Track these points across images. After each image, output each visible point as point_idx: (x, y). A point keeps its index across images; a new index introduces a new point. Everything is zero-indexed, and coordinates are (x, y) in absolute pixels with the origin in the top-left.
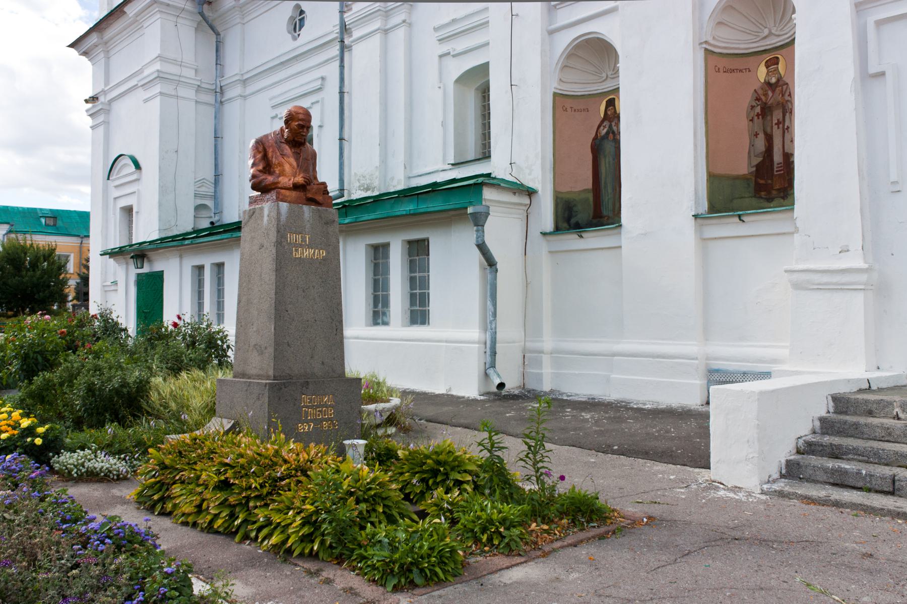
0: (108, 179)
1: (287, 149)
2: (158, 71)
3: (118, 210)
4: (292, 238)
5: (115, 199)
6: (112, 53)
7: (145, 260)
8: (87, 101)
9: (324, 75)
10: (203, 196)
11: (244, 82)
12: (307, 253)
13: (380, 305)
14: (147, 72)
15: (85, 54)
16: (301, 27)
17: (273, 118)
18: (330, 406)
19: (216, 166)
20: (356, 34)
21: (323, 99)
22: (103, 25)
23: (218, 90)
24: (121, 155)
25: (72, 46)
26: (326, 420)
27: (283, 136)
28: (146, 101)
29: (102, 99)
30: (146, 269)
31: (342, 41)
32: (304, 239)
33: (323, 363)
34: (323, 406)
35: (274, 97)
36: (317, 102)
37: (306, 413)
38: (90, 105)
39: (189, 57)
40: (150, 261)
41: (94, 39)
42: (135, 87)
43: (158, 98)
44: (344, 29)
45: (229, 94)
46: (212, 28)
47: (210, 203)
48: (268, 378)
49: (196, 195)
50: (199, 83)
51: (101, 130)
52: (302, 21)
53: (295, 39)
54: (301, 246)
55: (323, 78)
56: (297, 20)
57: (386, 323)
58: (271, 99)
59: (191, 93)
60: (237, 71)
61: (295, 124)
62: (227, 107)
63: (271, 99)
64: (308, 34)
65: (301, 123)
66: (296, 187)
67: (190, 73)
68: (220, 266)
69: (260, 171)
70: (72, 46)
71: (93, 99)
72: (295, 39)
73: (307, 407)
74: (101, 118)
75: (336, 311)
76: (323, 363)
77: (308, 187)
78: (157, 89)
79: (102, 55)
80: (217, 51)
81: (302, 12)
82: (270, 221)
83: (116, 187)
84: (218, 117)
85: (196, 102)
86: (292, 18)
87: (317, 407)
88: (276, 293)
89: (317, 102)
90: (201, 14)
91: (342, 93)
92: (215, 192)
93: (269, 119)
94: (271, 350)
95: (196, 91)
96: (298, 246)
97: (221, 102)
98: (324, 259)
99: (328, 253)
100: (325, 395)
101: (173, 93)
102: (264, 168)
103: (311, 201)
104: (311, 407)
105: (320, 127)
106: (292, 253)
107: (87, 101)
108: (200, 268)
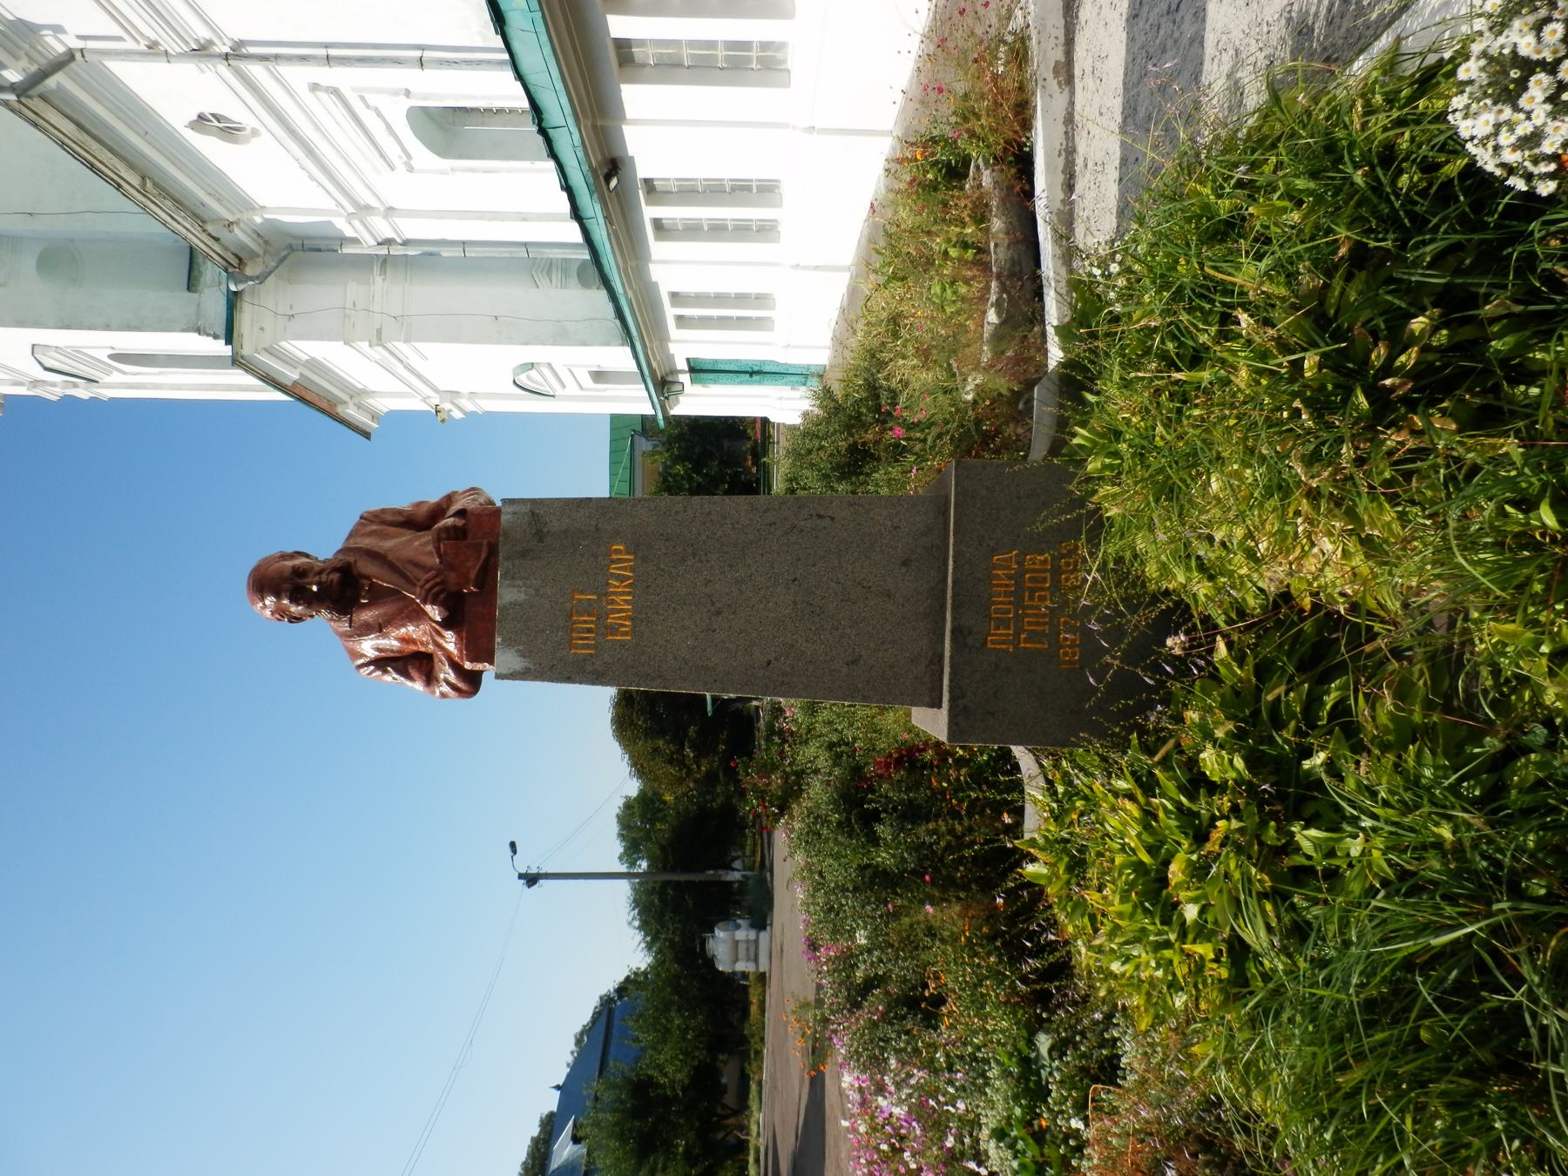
7: (670, 379)
12: (622, 601)
14: (377, 357)
16: (228, 120)
17: (411, 169)
20: (203, 33)
21: (354, 89)
22: (324, 405)
31: (226, 57)
32: (588, 609)
33: (905, 563)
36: (362, 98)
37: (1033, 636)
44: (202, 51)
52: (217, 117)
53: (255, 133)
54: (602, 616)
68: (675, 297)
73: (1017, 635)
76: (905, 563)
79: (370, 401)
83: (564, 386)
87: (1019, 603)
89: (362, 98)
98: (635, 547)
102: (420, 671)
103: (486, 580)
105: (408, 93)
106: (622, 644)
108: (680, 320)
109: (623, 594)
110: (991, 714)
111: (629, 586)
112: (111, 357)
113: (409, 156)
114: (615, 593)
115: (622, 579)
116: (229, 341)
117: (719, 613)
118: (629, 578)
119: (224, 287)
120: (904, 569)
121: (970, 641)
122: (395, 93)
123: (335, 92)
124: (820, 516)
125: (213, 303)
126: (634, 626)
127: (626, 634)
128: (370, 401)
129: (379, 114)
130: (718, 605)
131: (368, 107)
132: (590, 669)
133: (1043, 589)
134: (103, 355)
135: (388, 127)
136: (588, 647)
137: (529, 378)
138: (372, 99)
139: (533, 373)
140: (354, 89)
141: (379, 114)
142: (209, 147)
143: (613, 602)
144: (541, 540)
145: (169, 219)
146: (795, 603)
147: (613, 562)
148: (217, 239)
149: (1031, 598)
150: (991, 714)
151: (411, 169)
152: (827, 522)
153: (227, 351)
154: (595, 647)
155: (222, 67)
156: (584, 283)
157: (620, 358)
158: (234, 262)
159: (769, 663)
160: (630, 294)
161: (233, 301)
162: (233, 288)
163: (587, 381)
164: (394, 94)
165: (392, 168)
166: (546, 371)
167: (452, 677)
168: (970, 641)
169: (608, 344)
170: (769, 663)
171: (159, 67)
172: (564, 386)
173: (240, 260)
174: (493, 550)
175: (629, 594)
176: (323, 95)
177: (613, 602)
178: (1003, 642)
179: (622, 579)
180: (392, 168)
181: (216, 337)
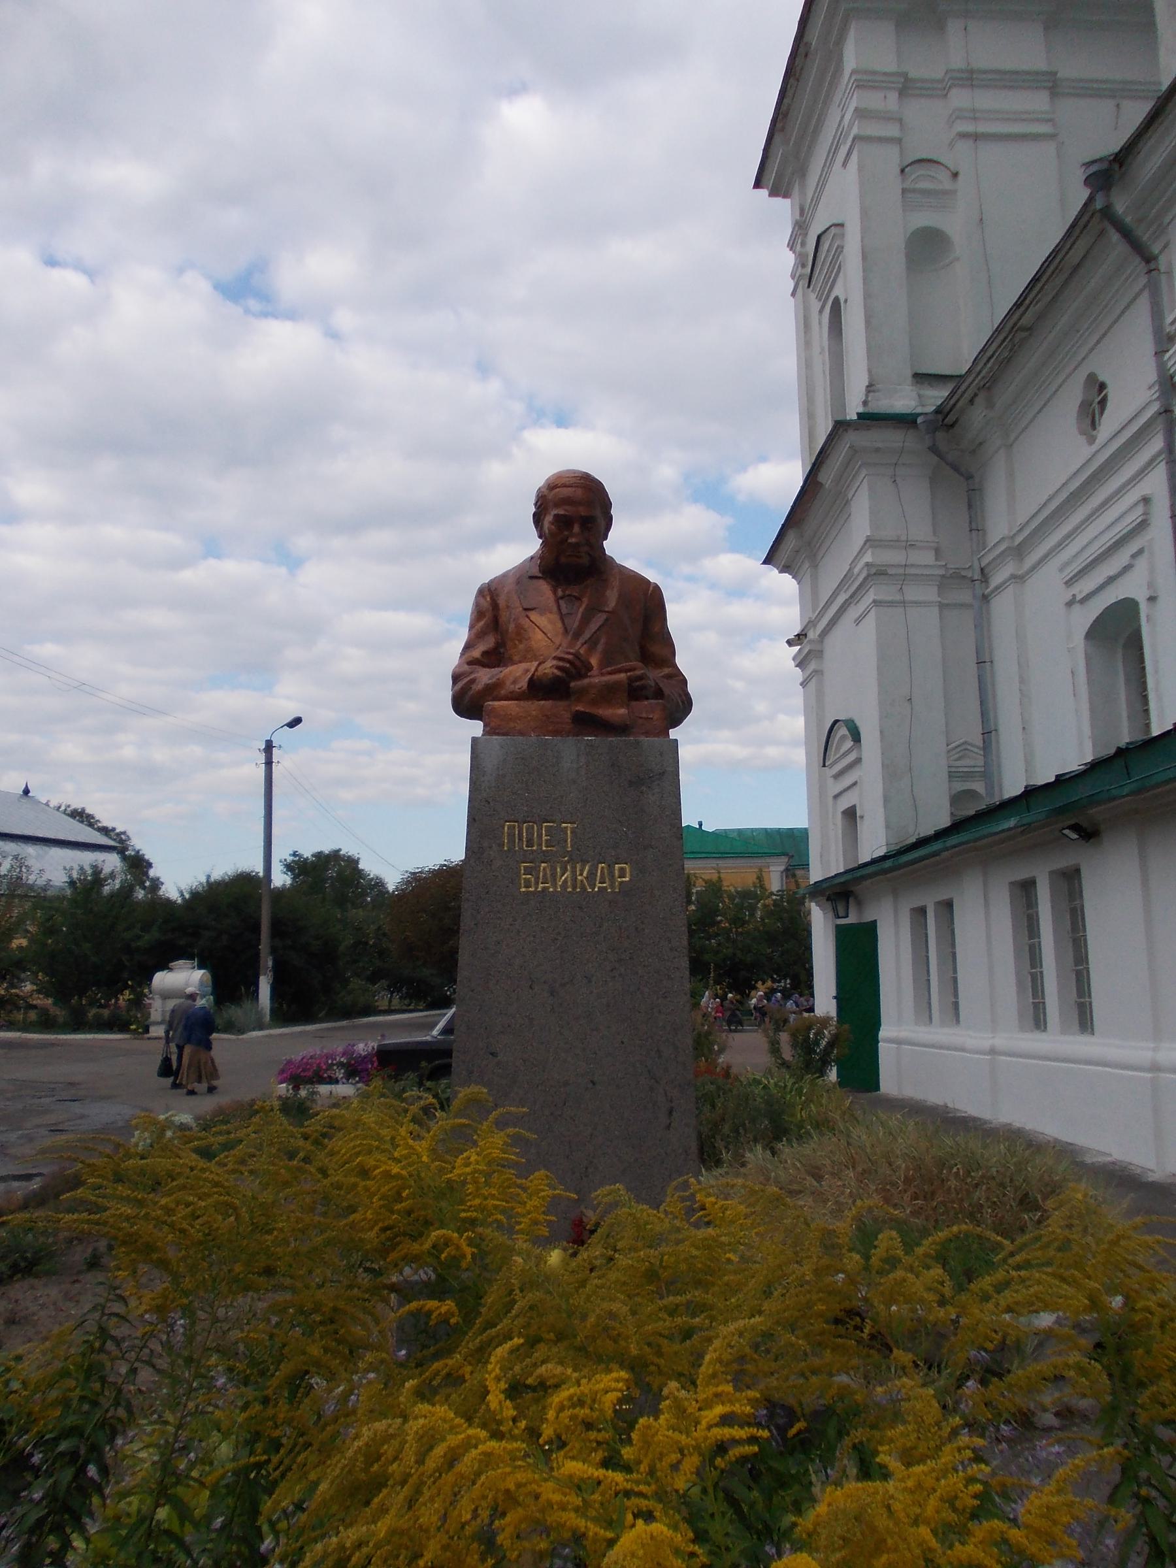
0: (824, 766)
2: (867, 564)
3: (839, 816)
5: (836, 797)
6: (819, 558)
7: (851, 900)
8: (790, 643)
10: (968, 776)
11: (1019, 552)
14: (856, 570)
15: (785, 569)
16: (1102, 413)
17: (1070, 604)
19: (984, 714)
24: (836, 722)
25: (765, 562)
28: (858, 621)
29: (812, 635)
30: (852, 919)
35: (1067, 564)
36: (1140, 552)
39: (921, 530)
40: (859, 904)
41: (791, 541)
43: (873, 613)
45: (996, 579)
46: (955, 468)
47: (979, 787)
49: (952, 776)
50: (942, 572)
51: (812, 684)
52: (1103, 403)
53: (1091, 440)
55: (1146, 500)
56: (1095, 405)
58: (1061, 570)
59: (930, 593)
60: (1006, 532)
63: (1061, 570)
64: (1109, 423)
65: (555, 512)
66: (538, 689)
67: (928, 558)
68: (949, 905)
71: (800, 638)
72: (1091, 440)
74: (812, 666)
78: (870, 596)
79: (807, 565)
80: (970, 506)
81: (1102, 386)
83: (837, 776)
84: (982, 625)
85: (942, 606)
86: (1085, 406)
89: (1140, 552)
90: (934, 449)
92: (986, 764)
95: (939, 587)
101: (898, 597)
102: (485, 654)
103: (586, 723)
105: (1152, 599)
108: (922, 911)
109: (575, 879)
111: (583, 888)
112: (837, 299)
116: (860, 416)
119: (919, 410)
122: (1150, 585)
123: (1143, 525)
124: (670, 1112)
125: (904, 400)
128: (807, 565)
129: (1127, 568)
131: (1134, 556)
132: (486, 844)
134: (838, 291)
135: (1111, 580)
137: (843, 737)
138: (1142, 564)
139: (849, 743)
141: (1127, 568)
142: (1072, 396)
144: (631, 783)
145: (989, 354)
147: (610, 867)
148: (971, 401)
153: (852, 416)
155: (1155, 407)
156: (957, 799)
157: (874, 843)
158: (950, 419)
160: (945, 854)
161: (906, 421)
162: (919, 420)
163: (845, 803)
165: (1069, 583)
166: (852, 757)
167: (478, 687)
169: (887, 827)
171: (1148, 346)
172: (837, 776)
173: (952, 426)
174: (621, 729)
175: (574, 887)
176: (1140, 510)
179: (591, 876)
180: (1069, 583)
181: (865, 403)
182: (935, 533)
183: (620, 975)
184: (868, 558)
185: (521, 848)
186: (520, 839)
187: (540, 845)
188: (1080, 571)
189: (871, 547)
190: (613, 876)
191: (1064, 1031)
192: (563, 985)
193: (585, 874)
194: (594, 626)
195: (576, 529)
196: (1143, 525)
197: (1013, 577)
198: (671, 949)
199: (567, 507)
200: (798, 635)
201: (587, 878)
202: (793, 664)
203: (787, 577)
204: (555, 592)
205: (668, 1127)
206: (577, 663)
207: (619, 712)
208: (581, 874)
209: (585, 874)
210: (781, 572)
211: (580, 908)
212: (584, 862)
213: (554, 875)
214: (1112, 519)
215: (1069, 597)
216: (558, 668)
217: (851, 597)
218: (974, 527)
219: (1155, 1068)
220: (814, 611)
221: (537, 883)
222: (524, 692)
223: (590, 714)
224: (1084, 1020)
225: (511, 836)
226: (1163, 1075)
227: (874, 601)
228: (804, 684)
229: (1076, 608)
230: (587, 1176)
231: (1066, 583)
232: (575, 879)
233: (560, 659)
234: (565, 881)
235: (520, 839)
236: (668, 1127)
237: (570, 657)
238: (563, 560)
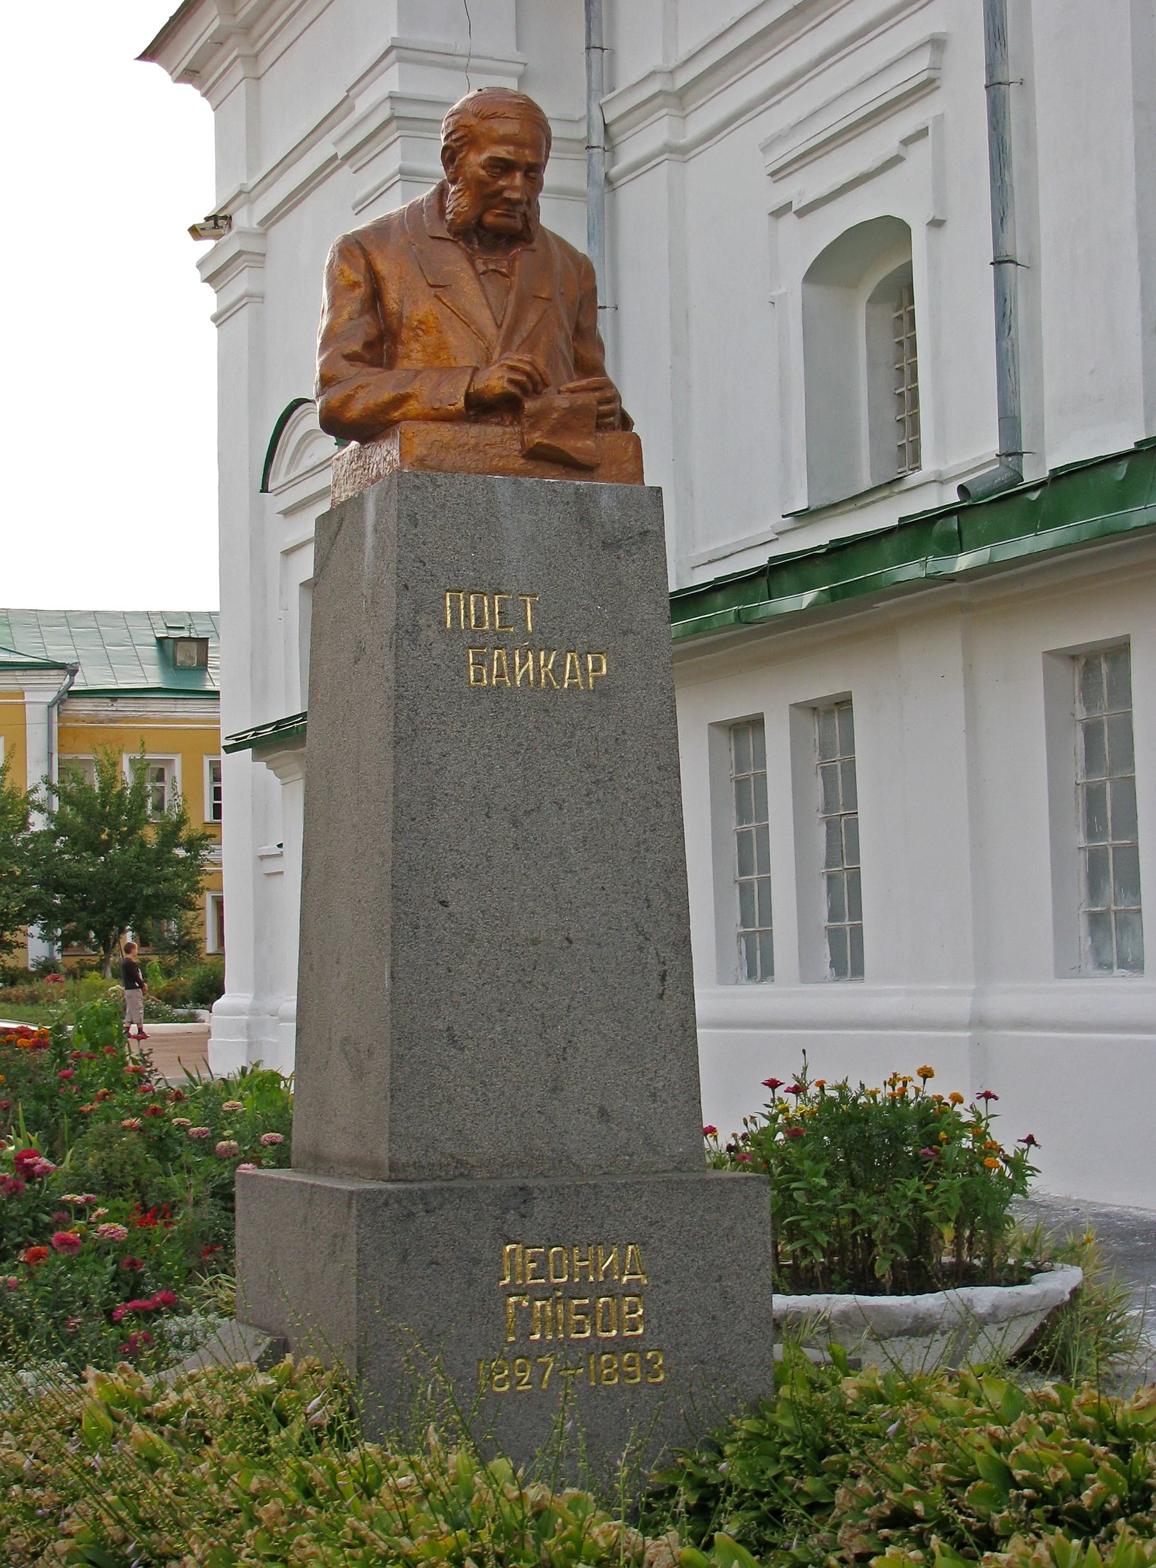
0: (264, 489)
1: (455, 262)
2: (392, 98)
3: (296, 591)
4: (459, 610)
5: (287, 553)
8: (195, 232)
9: (939, 28)
13: (1110, 888)
14: (362, 105)
15: (190, 75)
17: (778, 213)
18: (628, 1291)
23: (597, 139)
25: (149, 54)
26: (619, 1346)
27: (442, 210)
29: (243, 219)
33: (603, 1112)
34: (597, 1290)
38: (208, 245)
42: (331, 165)
45: (631, 151)
48: (372, 1169)
51: (243, 318)
55: (937, 43)
57: (1136, 965)
58: (766, 148)
60: (656, 61)
61: (475, 160)
62: (630, 196)
63: (766, 148)
69: (351, 358)
70: (149, 54)
71: (215, 224)
74: (241, 285)
75: (658, 899)
76: (604, 1114)
77: (529, 405)
82: (380, 548)
88: (397, 832)
89: (922, 133)
91: (993, 85)
93: (766, 218)
94: (382, 1060)
96: (482, 643)
97: (609, 181)
98: (603, 690)
99: (619, 663)
100: (607, 1243)
102: (368, 345)
104: (547, 1293)
105: (936, 224)
106: (462, 672)
107: (195, 232)
109: (537, 673)
110: (404, 1258)
111: (549, 683)
113: (802, 213)
114: (536, 660)
115: (559, 666)
117: (515, 823)
118: (561, 681)
120: (594, 1111)
121: (511, 1216)
123: (926, 87)
126: (488, 689)
127: (478, 679)
128: (239, 72)
130: (526, 822)
131: (906, 142)
133: (594, 1325)
136: (455, 618)
138: (920, 155)
140: (940, 120)
143: (524, 659)
146: (535, 942)
147: (582, 658)
149: (580, 1310)
150: (404, 1258)
151: (778, 213)
152: (656, 987)
154: (453, 630)
159: (444, 903)
164: (933, 189)
165: (777, 174)
168: (511, 1216)
170: (444, 903)
176: (924, 60)
177: (524, 659)
178: (512, 1270)
179: (559, 666)
180: (777, 174)
182: (519, 47)
183: (598, 800)
184: (391, 81)
185: (468, 627)
186: (467, 616)
187: (492, 624)
188: (802, 156)
189: (399, 60)
190: (586, 669)
191: (807, 975)
192: (528, 813)
193: (550, 667)
194: (532, 318)
195: (518, 179)
196: (926, 87)
197: (669, 149)
198: (659, 768)
199: (511, 148)
200: (214, 218)
201: (552, 670)
202: (197, 275)
203: (189, 91)
204: (473, 264)
205: (661, 996)
206: (537, 377)
207: (580, 445)
208: (546, 666)
209: (550, 667)
210: (178, 80)
211: (546, 711)
212: (549, 650)
213: (512, 667)
214: (871, 69)
215: (778, 201)
216: (511, 381)
217: (347, 157)
218: (595, 42)
219: (979, 1023)
220: (251, 169)
221: (490, 676)
222: (459, 411)
223: (548, 446)
224: (847, 958)
225: (455, 610)
226: (990, 1033)
227: (402, 171)
228: (219, 319)
229: (790, 218)
230: (565, 1059)
231: (772, 174)
232: (537, 673)
233: (512, 369)
234: (526, 675)
235: (467, 616)
236: (661, 996)
237: (528, 368)
238: (489, 219)
